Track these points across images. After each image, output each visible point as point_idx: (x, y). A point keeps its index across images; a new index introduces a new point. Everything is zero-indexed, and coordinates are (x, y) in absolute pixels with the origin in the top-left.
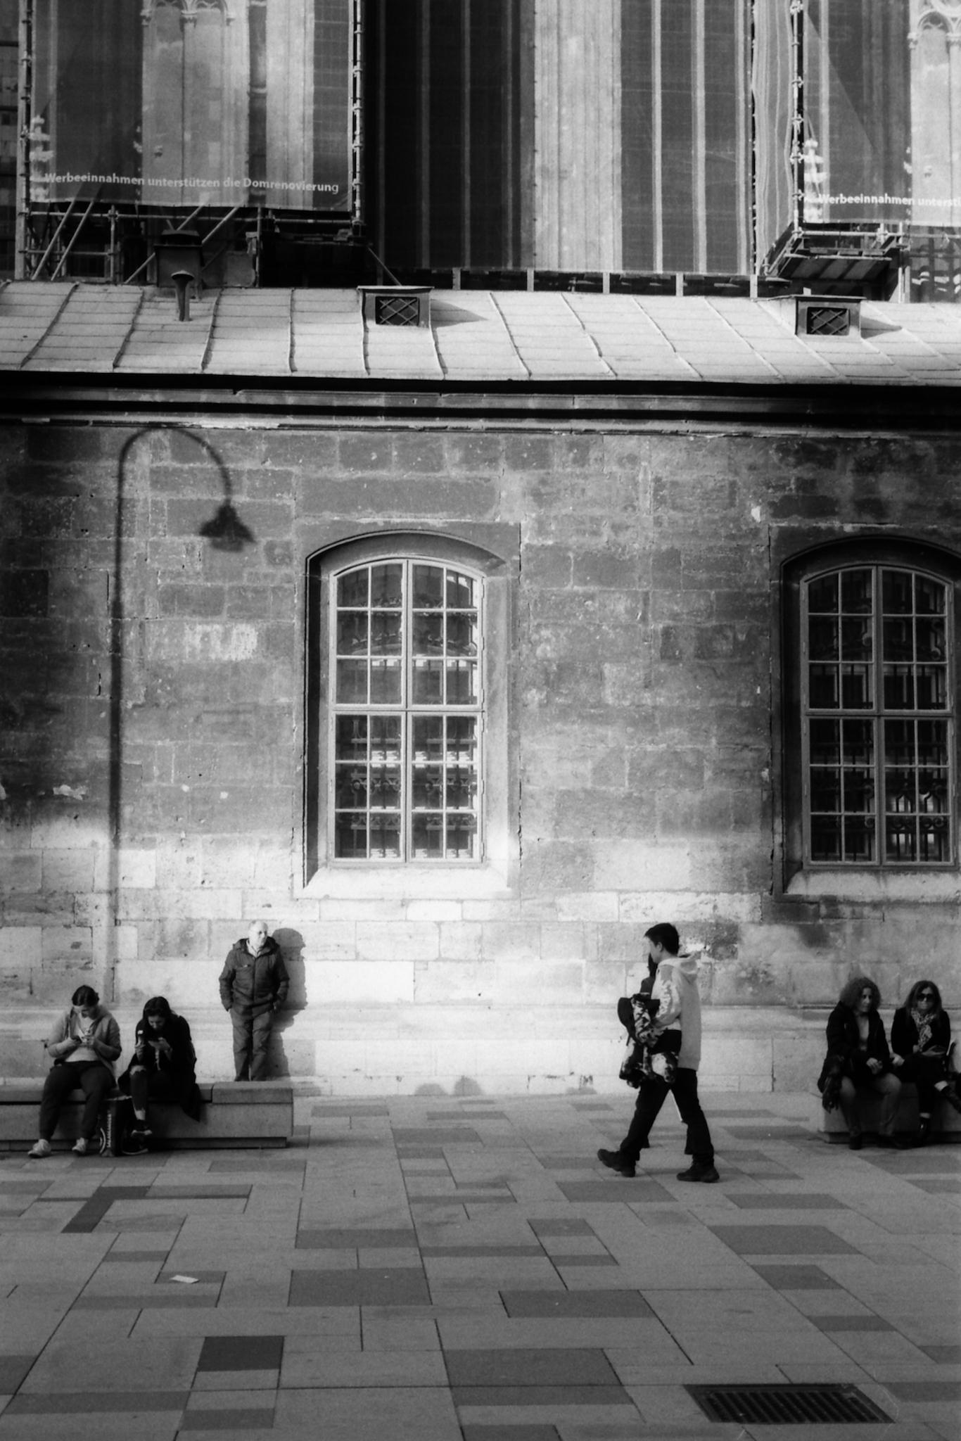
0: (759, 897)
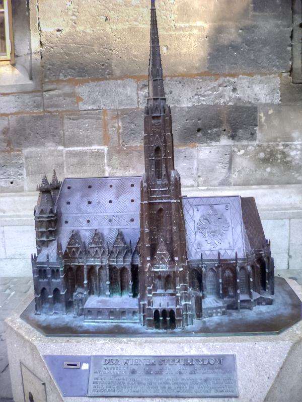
0: (278, 79)
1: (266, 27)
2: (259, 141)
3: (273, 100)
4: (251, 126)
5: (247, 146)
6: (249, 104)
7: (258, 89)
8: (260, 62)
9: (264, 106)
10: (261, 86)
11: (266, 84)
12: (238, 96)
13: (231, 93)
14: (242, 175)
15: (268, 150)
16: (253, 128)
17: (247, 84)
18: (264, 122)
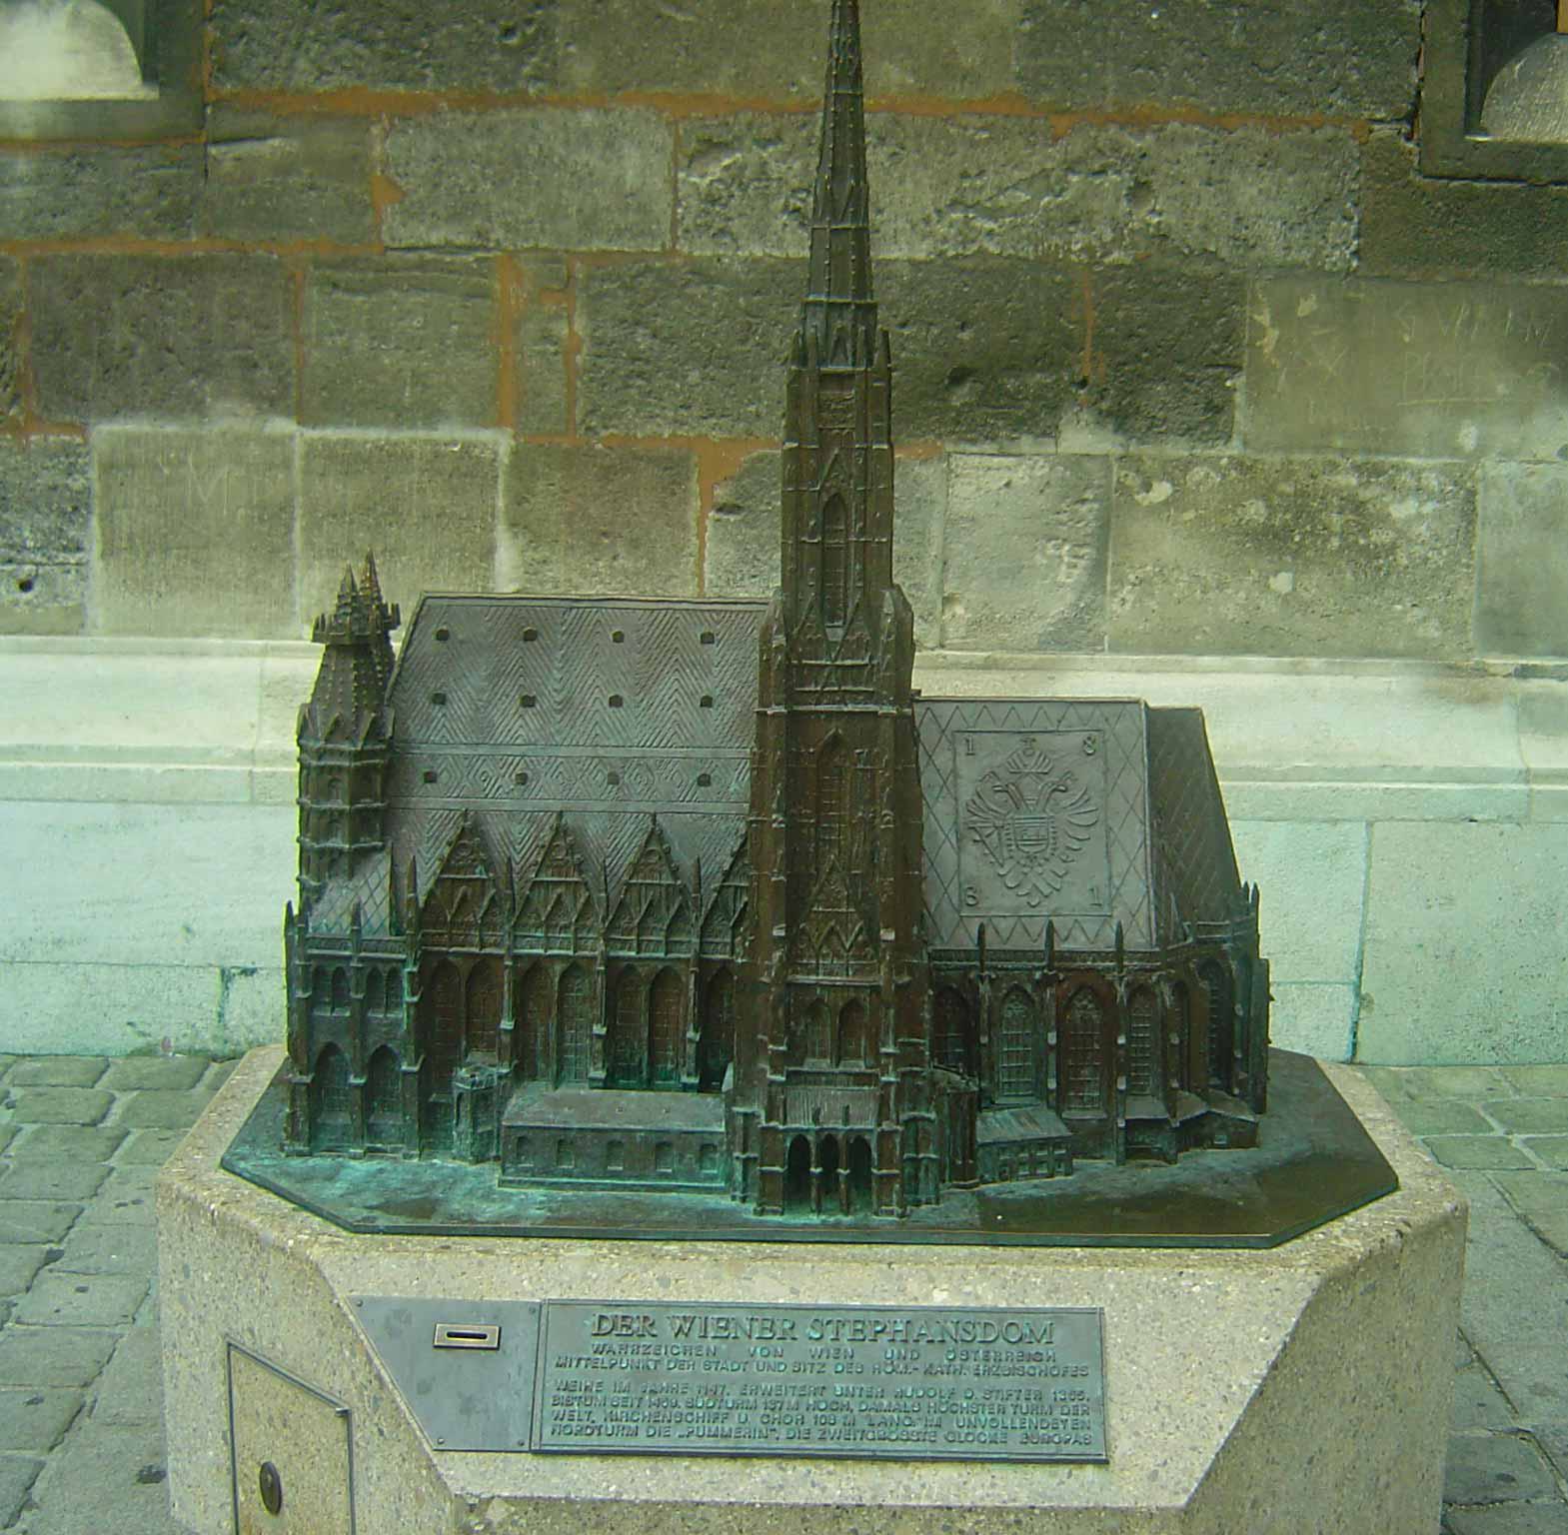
2: (1245, 444)
4: (1210, 371)
5: (1188, 465)
7: (1254, 191)
9: (1277, 278)
11: (1292, 173)
13: (1124, 205)
15: (1287, 488)
16: (1219, 380)
17: (1202, 162)
18: (1277, 350)
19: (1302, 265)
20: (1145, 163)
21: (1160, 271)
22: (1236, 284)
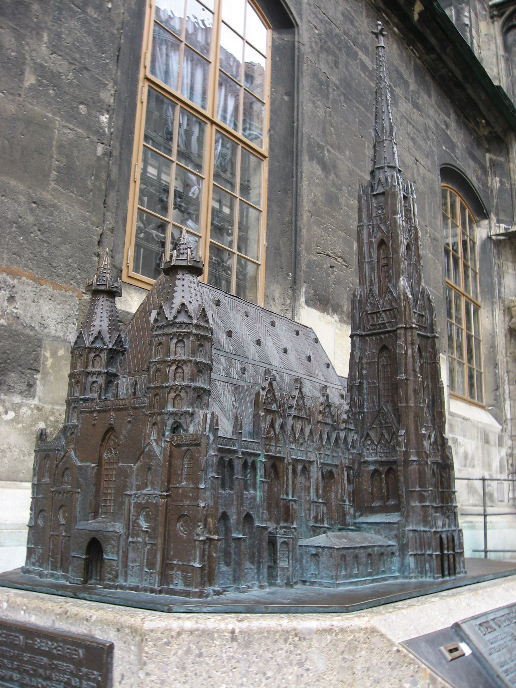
1: (70, 215)
2: (40, 400)
3: (66, 333)
4: (29, 371)
5: (20, 406)
6: (31, 330)
7: (47, 308)
8: (55, 265)
9: (53, 340)
10: (52, 305)
11: (59, 304)
12: (16, 311)
13: (6, 304)
14: (6, 460)
15: (52, 419)
16: (32, 375)
17: (32, 294)
18: (51, 367)
19: (60, 338)
20: (14, 290)
21: (16, 331)
22: (40, 340)
